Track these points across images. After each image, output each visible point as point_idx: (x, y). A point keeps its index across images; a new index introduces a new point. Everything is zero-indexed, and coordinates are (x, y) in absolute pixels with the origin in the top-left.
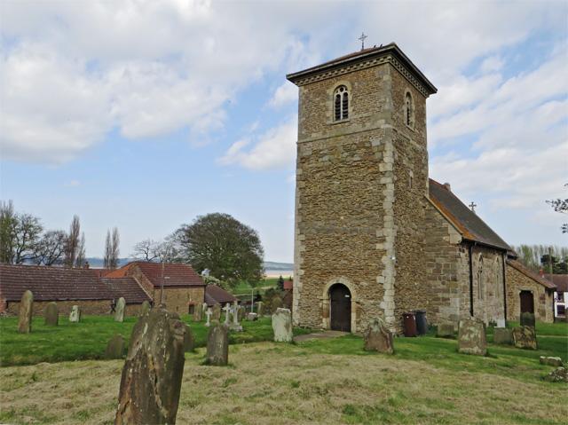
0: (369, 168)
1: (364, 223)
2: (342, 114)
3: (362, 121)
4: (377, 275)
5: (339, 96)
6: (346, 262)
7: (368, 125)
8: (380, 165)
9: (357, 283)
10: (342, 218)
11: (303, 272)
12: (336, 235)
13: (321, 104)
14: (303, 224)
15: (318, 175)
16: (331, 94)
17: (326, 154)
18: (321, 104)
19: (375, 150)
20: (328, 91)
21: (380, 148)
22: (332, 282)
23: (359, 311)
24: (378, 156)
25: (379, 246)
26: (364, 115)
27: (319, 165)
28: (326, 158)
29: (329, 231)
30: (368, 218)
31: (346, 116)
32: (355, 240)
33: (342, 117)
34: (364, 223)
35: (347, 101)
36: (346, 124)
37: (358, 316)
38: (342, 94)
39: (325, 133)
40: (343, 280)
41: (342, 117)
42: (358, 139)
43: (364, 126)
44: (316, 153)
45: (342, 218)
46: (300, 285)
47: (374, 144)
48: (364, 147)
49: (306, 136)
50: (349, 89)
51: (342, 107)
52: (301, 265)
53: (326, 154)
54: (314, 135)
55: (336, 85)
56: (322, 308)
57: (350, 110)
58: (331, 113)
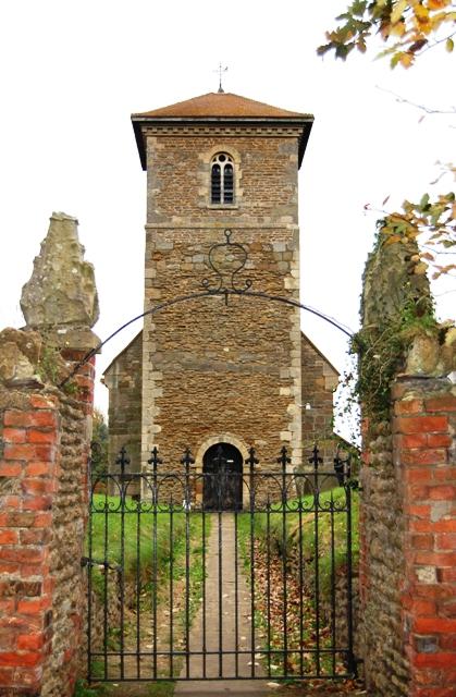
0: (268, 281)
1: (261, 359)
2: (222, 196)
4: (280, 430)
5: (217, 167)
6: (233, 412)
7: (267, 221)
8: (286, 280)
10: (227, 350)
11: (159, 428)
12: (217, 374)
13: (190, 174)
14: (159, 356)
15: (185, 282)
16: (206, 161)
17: (198, 252)
18: (190, 174)
20: (201, 156)
21: (286, 256)
22: (211, 442)
24: (282, 266)
25: (284, 391)
26: (261, 204)
27: (186, 267)
28: (199, 258)
29: (204, 367)
31: (229, 198)
32: (246, 381)
33: (222, 200)
34: (261, 359)
36: (232, 213)
38: (222, 165)
40: (228, 438)
41: (222, 200)
42: (252, 238)
43: (261, 220)
44: (183, 250)
45: (227, 350)
47: (276, 249)
48: (261, 251)
51: (222, 184)
52: (157, 417)
53: (198, 252)
55: (216, 149)
58: (205, 191)
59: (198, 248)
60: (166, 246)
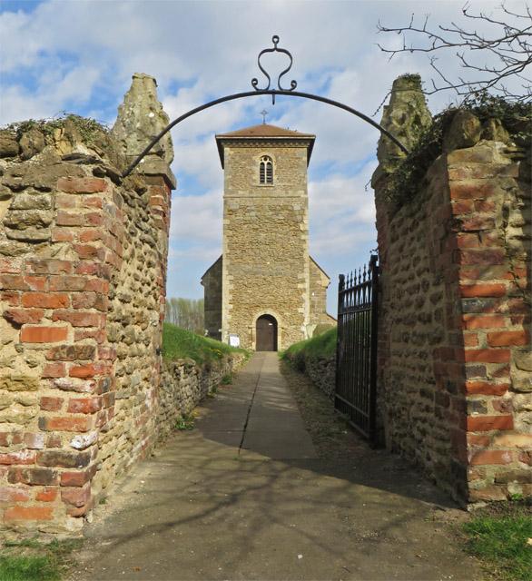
3: (285, 189)
5: (262, 164)
7: (290, 193)
9: (281, 313)
11: (232, 306)
15: (246, 226)
19: (297, 213)
21: (301, 212)
23: (283, 337)
24: (299, 218)
25: (300, 286)
28: (253, 214)
29: (255, 273)
30: (291, 264)
31: (270, 181)
35: (271, 169)
37: (283, 337)
38: (266, 163)
39: (251, 192)
40: (269, 312)
43: (287, 193)
44: (245, 209)
46: (230, 317)
49: (232, 192)
50: (274, 160)
54: (240, 192)
56: (251, 335)
57: (275, 178)
58: (257, 177)
59: (253, 208)
60: (234, 205)
